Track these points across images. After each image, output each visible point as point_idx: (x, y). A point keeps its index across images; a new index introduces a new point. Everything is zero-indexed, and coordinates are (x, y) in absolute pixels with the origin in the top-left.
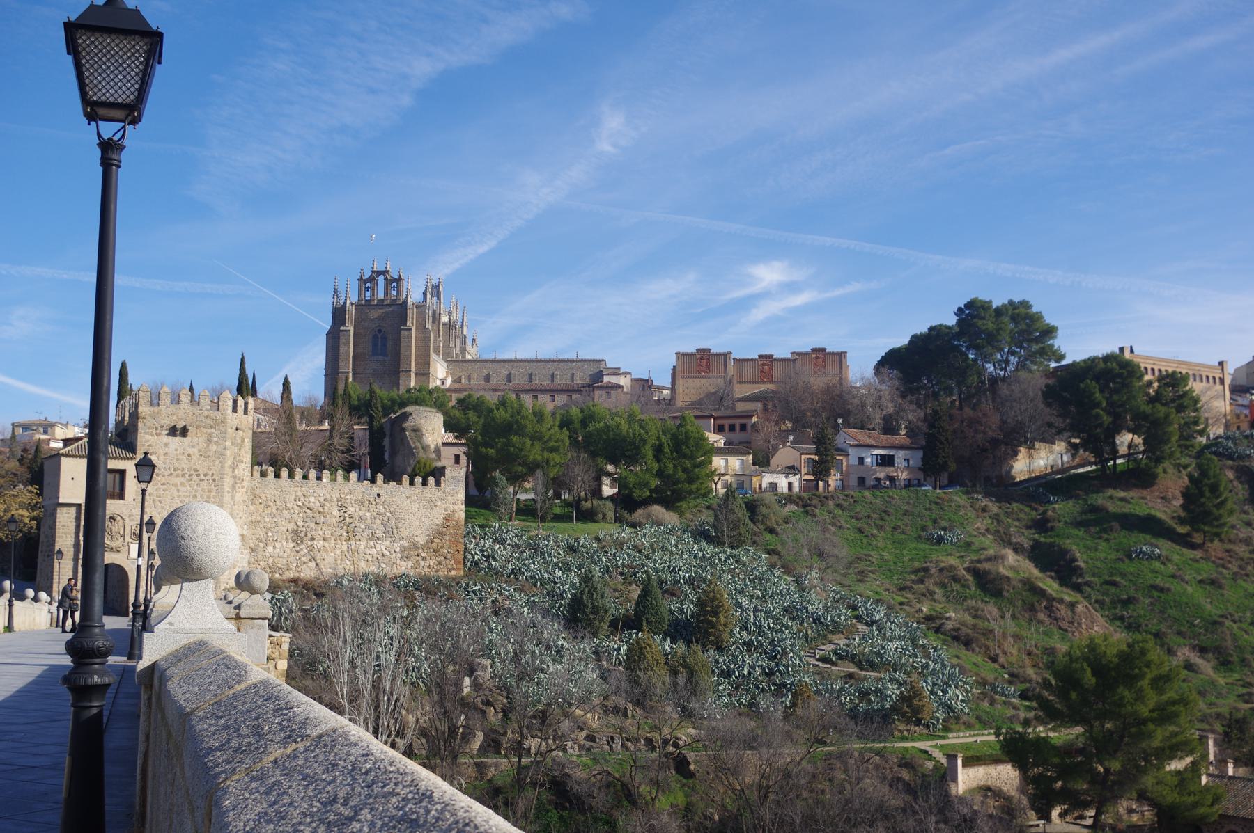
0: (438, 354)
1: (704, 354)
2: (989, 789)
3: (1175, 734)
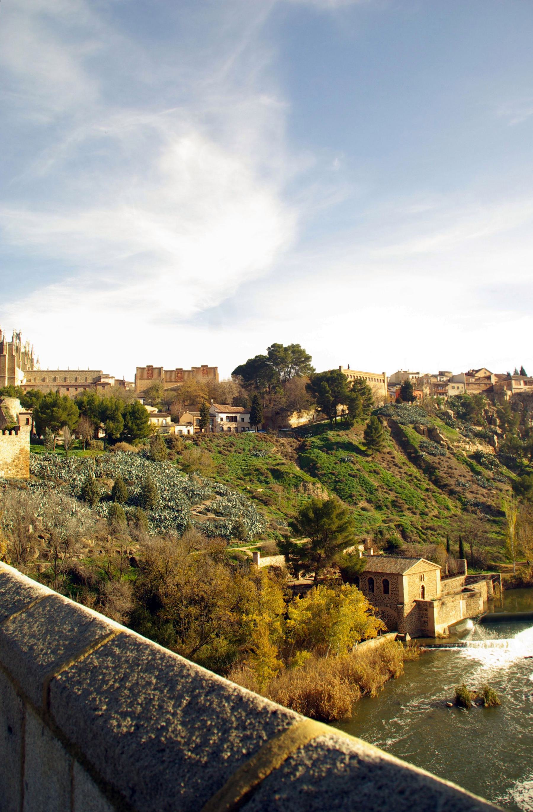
0: (19, 368)
1: (150, 368)
2: (271, 566)
3: (346, 537)
